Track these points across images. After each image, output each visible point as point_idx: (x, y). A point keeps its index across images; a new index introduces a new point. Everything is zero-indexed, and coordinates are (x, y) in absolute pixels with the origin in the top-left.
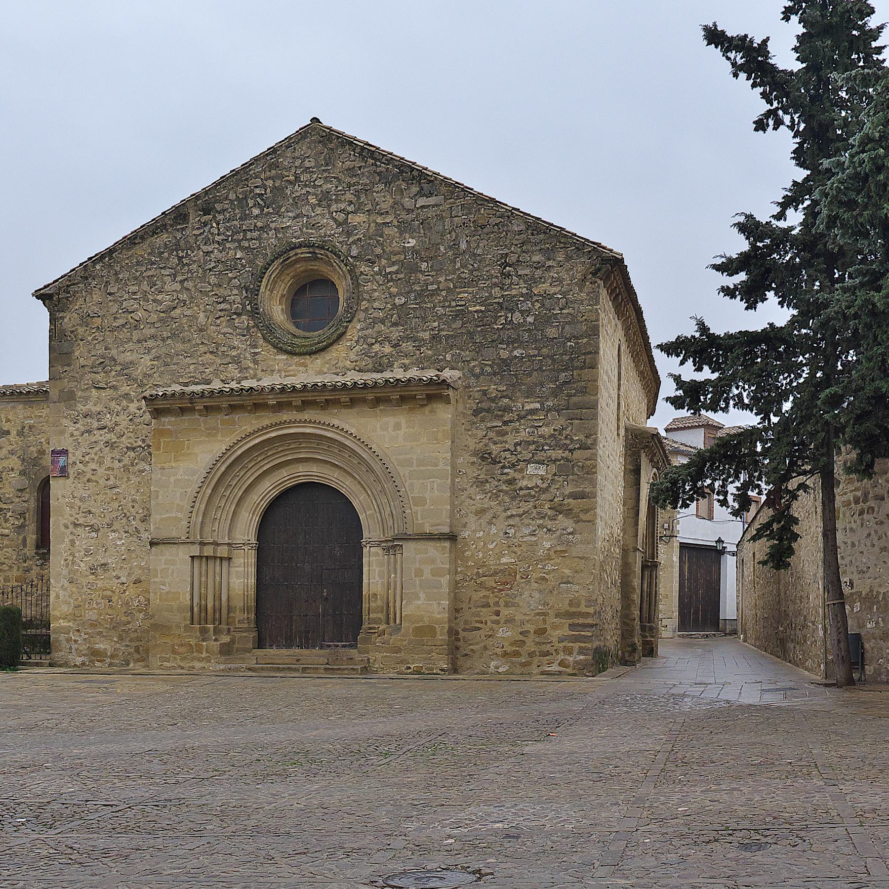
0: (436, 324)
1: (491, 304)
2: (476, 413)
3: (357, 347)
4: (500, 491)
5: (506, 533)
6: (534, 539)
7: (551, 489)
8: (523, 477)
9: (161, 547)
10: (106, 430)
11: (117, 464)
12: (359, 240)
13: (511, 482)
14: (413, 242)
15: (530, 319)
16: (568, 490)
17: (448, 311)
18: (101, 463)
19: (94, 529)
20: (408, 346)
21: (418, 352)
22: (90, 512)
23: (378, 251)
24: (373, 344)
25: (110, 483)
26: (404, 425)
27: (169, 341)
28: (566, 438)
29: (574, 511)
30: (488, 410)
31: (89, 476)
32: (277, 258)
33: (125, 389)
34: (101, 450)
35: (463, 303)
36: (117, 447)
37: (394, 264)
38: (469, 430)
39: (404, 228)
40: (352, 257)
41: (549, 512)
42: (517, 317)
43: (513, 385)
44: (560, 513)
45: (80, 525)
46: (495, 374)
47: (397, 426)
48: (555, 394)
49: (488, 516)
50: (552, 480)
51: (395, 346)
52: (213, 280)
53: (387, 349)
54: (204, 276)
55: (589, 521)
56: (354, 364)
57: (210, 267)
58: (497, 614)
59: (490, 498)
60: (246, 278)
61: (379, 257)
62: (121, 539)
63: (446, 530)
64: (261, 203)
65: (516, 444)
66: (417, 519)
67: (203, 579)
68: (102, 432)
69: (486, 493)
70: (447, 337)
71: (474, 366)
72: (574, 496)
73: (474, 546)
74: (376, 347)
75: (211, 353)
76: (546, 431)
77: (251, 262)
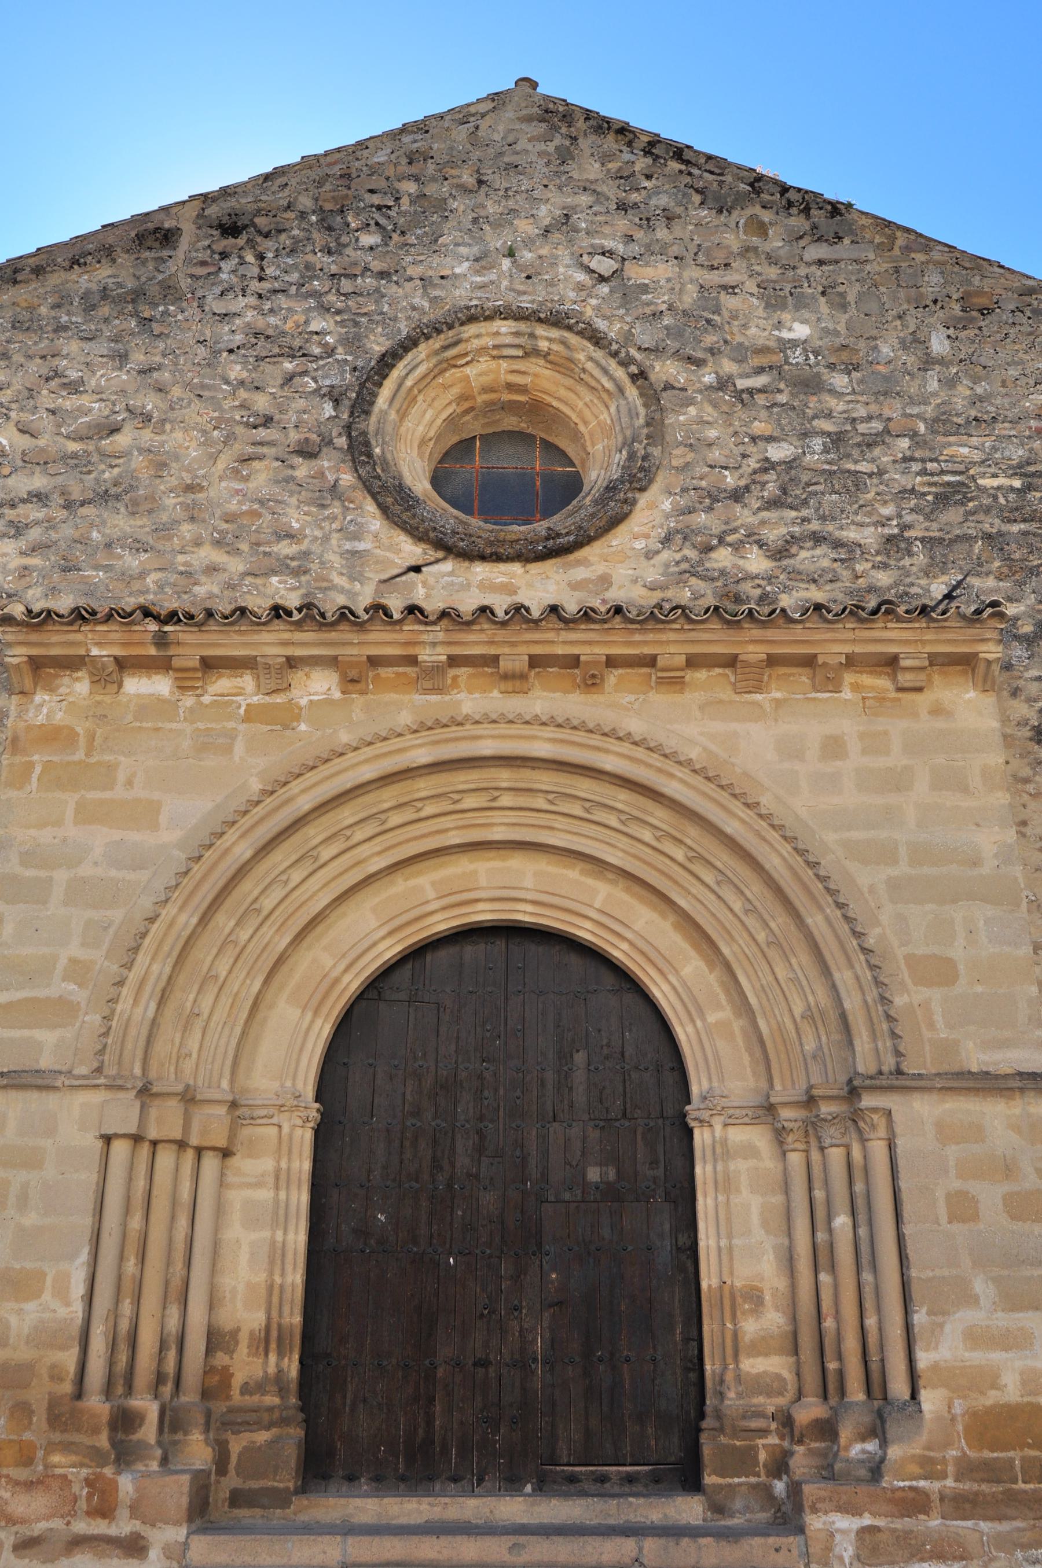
0: (888, 510)
12: (657, 315)
14: (801, 331)
17: (924, 484)
23: (710, 339)
24: (710, 549)
26: (854, 746)
32: (428, 337)
35: (962, 468)
37: (760, 370)
38: (1026, 781)
51: (780, 553)
52: (236, 371)
53: (756, 562)
57: (234, 346)
61: (711, 351)
66: (931, 1025)
74: (722, 558)
75: (218, 543)
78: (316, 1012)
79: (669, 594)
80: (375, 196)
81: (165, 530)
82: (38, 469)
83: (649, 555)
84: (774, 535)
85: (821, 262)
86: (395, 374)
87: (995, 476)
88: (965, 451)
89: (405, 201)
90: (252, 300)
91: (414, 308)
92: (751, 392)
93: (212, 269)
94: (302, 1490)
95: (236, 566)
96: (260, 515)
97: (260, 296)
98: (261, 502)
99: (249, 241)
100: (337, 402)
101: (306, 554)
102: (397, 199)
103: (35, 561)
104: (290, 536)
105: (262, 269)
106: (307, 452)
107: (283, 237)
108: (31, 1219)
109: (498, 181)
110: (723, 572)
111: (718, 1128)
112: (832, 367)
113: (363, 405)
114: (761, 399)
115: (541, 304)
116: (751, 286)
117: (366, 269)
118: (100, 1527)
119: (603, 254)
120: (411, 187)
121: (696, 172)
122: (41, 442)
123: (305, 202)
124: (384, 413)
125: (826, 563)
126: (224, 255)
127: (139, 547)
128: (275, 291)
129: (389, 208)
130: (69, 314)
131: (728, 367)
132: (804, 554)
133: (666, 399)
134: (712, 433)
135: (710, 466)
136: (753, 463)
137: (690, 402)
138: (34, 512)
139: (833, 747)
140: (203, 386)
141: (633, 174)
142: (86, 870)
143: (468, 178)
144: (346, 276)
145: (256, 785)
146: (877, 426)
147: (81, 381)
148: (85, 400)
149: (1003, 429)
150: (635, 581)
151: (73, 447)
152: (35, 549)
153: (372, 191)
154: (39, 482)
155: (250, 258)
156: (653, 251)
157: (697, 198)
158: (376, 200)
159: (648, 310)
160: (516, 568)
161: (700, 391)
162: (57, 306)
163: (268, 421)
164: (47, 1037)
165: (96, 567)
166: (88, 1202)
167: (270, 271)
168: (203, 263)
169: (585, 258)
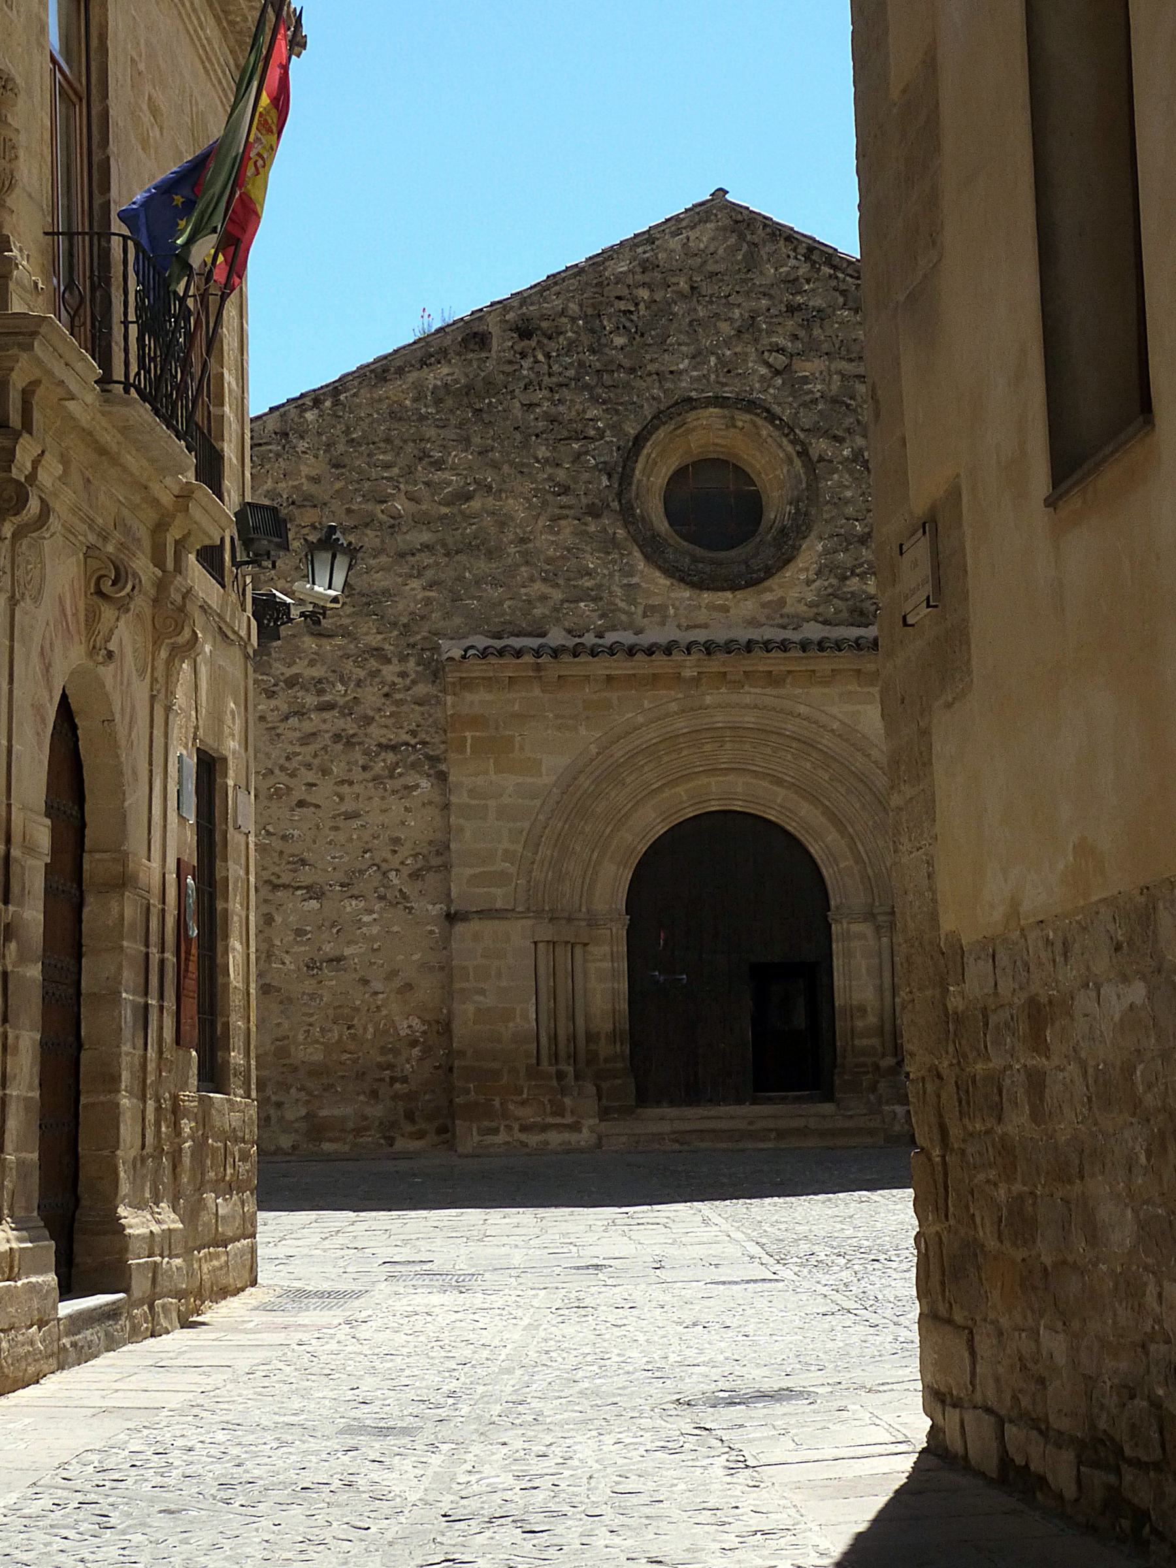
3: (818, 583)
9: (475, 925)
10: (336, 713)
11: (358, 775)
12: (815, 401)
19: (314, 892)
22: (303, 862)
24: (846, 578)
25: (347, 806)
31: (300, 793)
33: (374, 640)
34: (325, 748)
36: (360, 743)
40: (802, 430)
45: (285, 886)
52: (542, 452)
56: (815, 610)
61: (848, 430)
62: (371, 912)
68: (326, 715)
74: (854, 584)
75: (544, 580)
78: (625, 867)
79: (821, 609)
80: (622, 302)
81: (511, 571)
82: (424, 528)
83: (808, 583)
89: (642, 306)
90: (546, 393)
91: (654, 398)
93: (516, 367)
94: (637, 1106)
95: (557, 595)
96: (569, 559)
97: (551, 390)
98: (569, 550)
99: (539, 342)
100: (610, 476)
101: (599, 586)
102: (637, 305)
104: (589, 574)
105: (550, 367)
106: (594, 512)
107: (561, 339)
108: (504, 984)
109: (706, 289)
110: (852, 593)
111: (845, 925)
113: (625, 478)
115: (738, 394)
117: (620, 366)
118: (558, 1120)
119: (777, 351)
120: (644, 294)
123: (573, 307)
124: (640, 481)
126: (523, 355)
127: (496, 584)
128: (562, 385)
129: (631, 312)
130: (426, 406)
133: (820, 469)
134: (849, 494)
135: (848, 519)
137: (836, 471)
140: (523, 465)
141: (797, 279)
142: (506, 800)
143: (683, 285)
144: (607, 371)
148: (446, 475)
150: (799, 601)
151: (445, 510)
152: (431, 586)
153: (619, 298)
154: (426, 537)
155: (541, 357)
156: (811, 349)
157: (841, 300)
158: (622, 305)
159: (808, 398)
161: (841, 463)
162: (415, 400)
163: (566, 490)
164: (499, 892)
165: (473, 598)
167: (556, 368)
168: (510, 362)
169: (766, 354)
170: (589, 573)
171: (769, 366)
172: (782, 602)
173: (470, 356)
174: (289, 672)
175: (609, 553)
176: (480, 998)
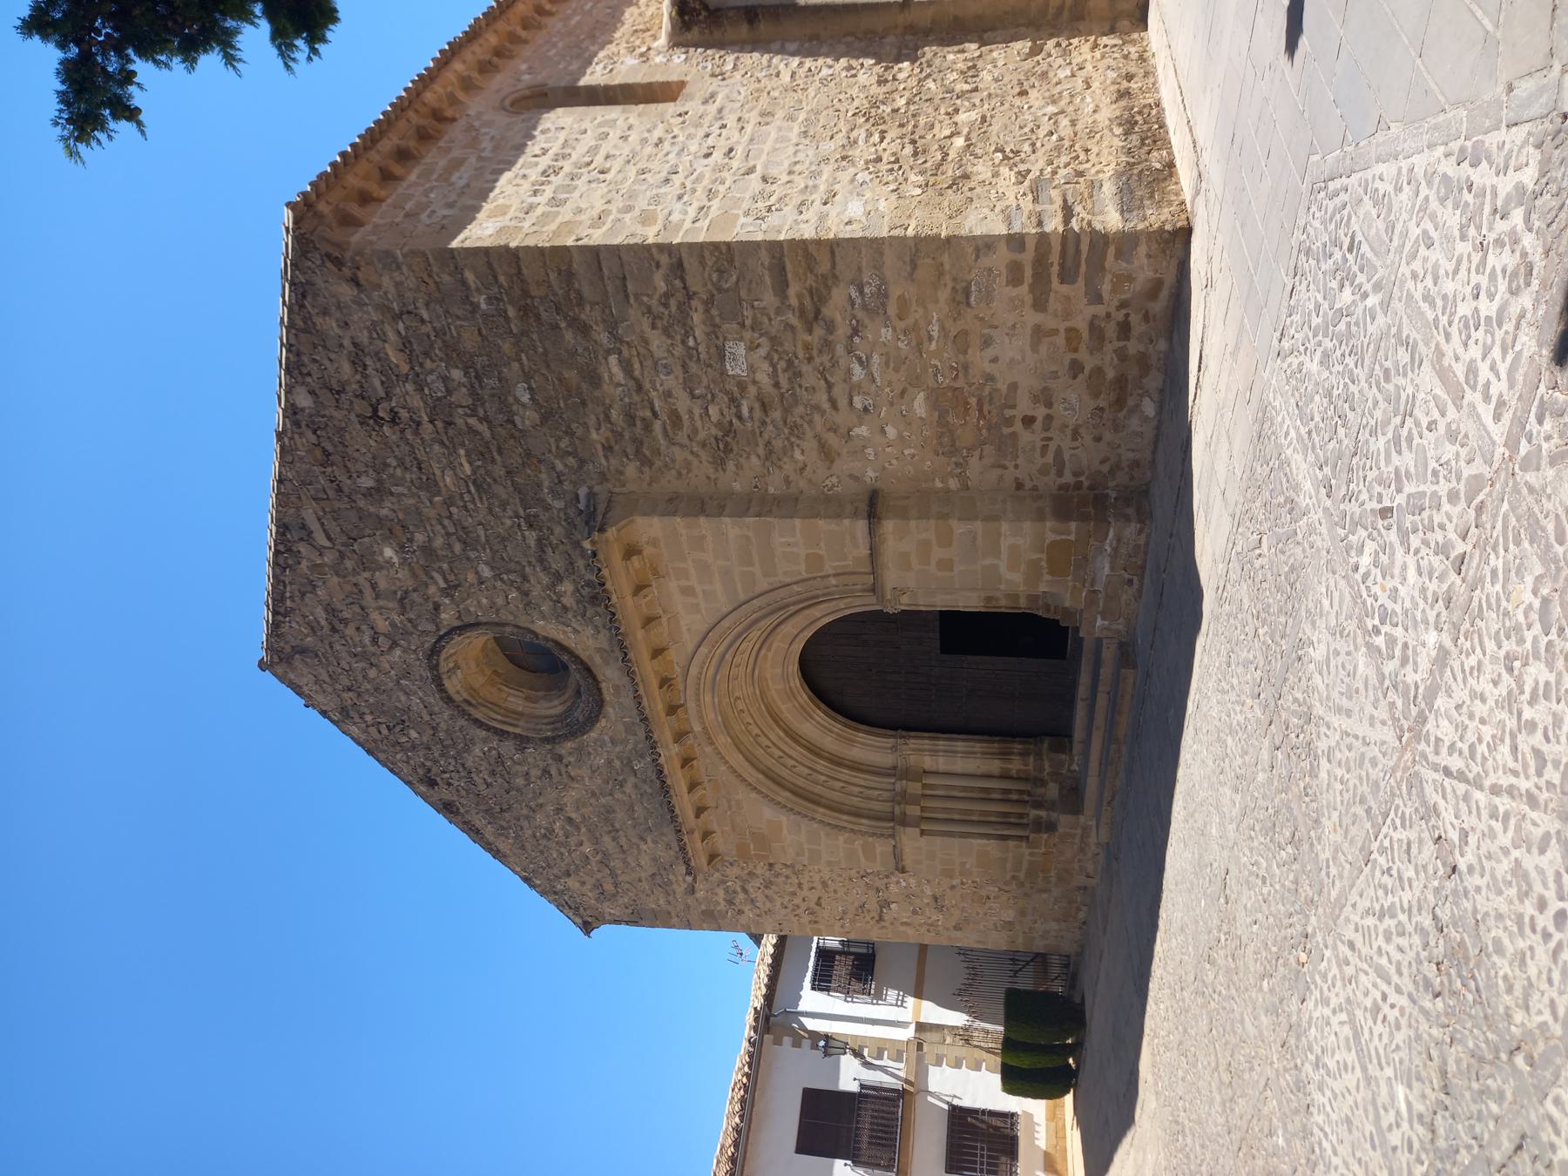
1: (451, 440)
2: (646, 462)
4: (785, 422)
5: (866, 409)
6: (876, 359)
7: (773, 332)
8: (754, 382)
12: (410, 621)
13: (765, 408)
14: (388, 552)
15: (457, 374)
16: (769, 299)
18: (794, 894)
19: (885, 904)
20: (556, 562)
21: (561, 547)
22: (862, 906)
24: (565, 608)
27: (617, 826)
28: (666, 305)
29: (814, 285)
30: (638, 443)
31: (812, 905)
38: (680, 474)
39: (367, 562)
41: (819, 331)
42: (462, 397)
43: (584, 403)
44: (818, 312)
46: (570, 433)
47: (687, 591)
48: (584, 330)
49: (832, 440)
50: (753, 329)
51: (558, 578)
52: (520, 781)
53: (566, 587)
54: (518, 790)
55: (833, 253)
56: (601, 629)
58: (1028, 421)
59: (798, 437)
60: (508, 747)
62: (898, 882)
63: (861, 526)
64: (398, 728)
65: (693, 396)
67: (956, 817)
69: (792, 444)
70: (525, 509)
71: (566, 465)
72: (781, 285)
73: (894, 462)
74: (568, 601)
75: (621, 786)
76: (657, 342)
77: (485, 741)
83: (576, 631)
84: (546, 580)
85: (329, 538)
86: (498, 726)
87: (461, 465)
88: (448, 480)
92: (446, 580)
95: (631, 780)
98: (593, 772)
103: (649, 840)
112: (411, 540)
114: (451, 578)
116: (367, 574)
121: (288, 595)
122: (584, 838)
125: (557, 557)
126: (449, 784)
131: (432, 590)
132: (554, 566)
136: (499, 584)
138: (623, 841)
139: (687, 591)
145: (753, 795)
146: (446, 522)
147: (546, 829)
149: (421, 455)
151: (583, 830)
154: (607, 839)
155: (447, 775)
158: (385, 731)
160: (603, 685)
164: (879, 849)
166: (946, 839)
170: (609, 762)
171: (391, 648)
172: (599, 650)
173: (462, 810)
174: (723, 903)
175: (589, 754)
176: (968, 866)
